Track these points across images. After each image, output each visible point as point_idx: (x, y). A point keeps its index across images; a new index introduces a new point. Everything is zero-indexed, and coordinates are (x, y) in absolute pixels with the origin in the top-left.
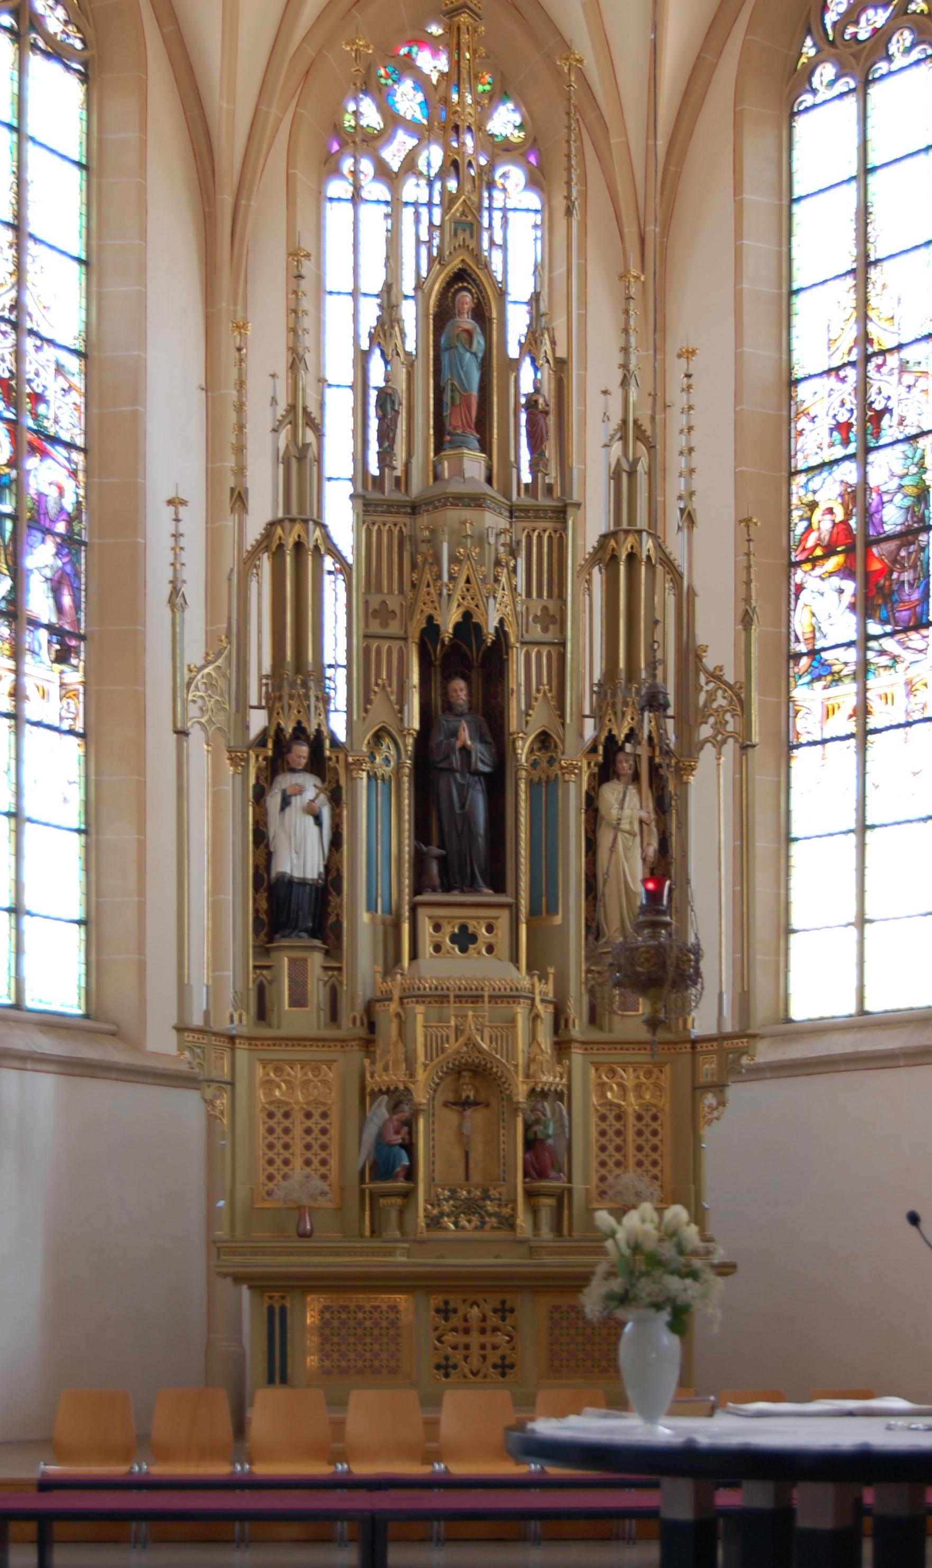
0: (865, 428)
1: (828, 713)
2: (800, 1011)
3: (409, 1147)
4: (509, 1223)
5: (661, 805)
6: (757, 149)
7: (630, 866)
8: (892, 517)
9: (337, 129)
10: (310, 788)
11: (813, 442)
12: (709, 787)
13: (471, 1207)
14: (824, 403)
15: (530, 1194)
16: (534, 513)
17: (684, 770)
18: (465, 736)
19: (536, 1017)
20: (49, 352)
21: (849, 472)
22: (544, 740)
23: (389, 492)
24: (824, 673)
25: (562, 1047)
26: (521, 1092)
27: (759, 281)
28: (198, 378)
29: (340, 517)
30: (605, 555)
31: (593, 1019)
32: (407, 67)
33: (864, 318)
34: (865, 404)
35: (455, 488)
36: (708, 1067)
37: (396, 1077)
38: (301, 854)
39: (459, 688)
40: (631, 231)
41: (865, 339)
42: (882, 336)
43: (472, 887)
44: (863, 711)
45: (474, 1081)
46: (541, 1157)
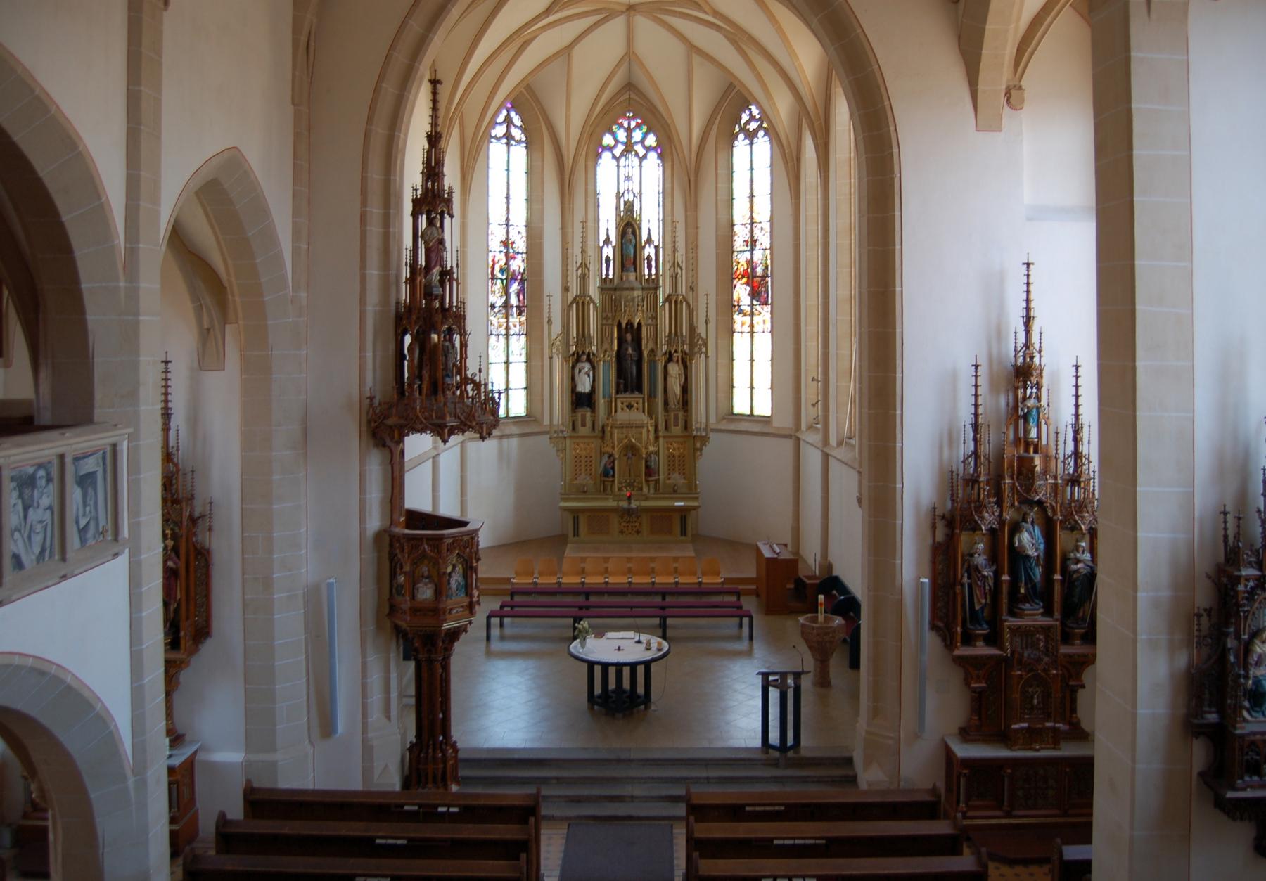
0: (752, 243)
1: (743, 325)
2: (736, 411)
3: (613, 469)
4: (641, 489)
5: (685, 367)
6: (722, 156)
7: (676, 388)
8: (759, 271)
9: (601, 145)
10: (587, 366)
11: (739, 244)
12: (699, 365)
13: (630, 485)
14: (741, 234)
15: (647, 481)
16: (649, 289)
17: (691, 360)
18: (630, 351)
19: (648, 431)
20: (517, 229)
21: (748, 255)
22: (652, 351)
23: (608, 285)
24: (741, 312)
25: (657, 438)
26: (644, 451)
27: (723, 196)
28: (559, 225)
29: (594, 291)
30: (668, 299)
31: (666, 428)
32: (621, 125)
33: (752, 212)
34: (752, 237)
35: (626, 285)
36: (698, 445)
37: (609, 449)
38: (584, 386)
39: (629, 337)
40: (686, 179)
41: (752, 217)
42: (757, 218)
43: (632, 392)
44: (752, 326)
45: (631, 450)
46: (649, 471)
